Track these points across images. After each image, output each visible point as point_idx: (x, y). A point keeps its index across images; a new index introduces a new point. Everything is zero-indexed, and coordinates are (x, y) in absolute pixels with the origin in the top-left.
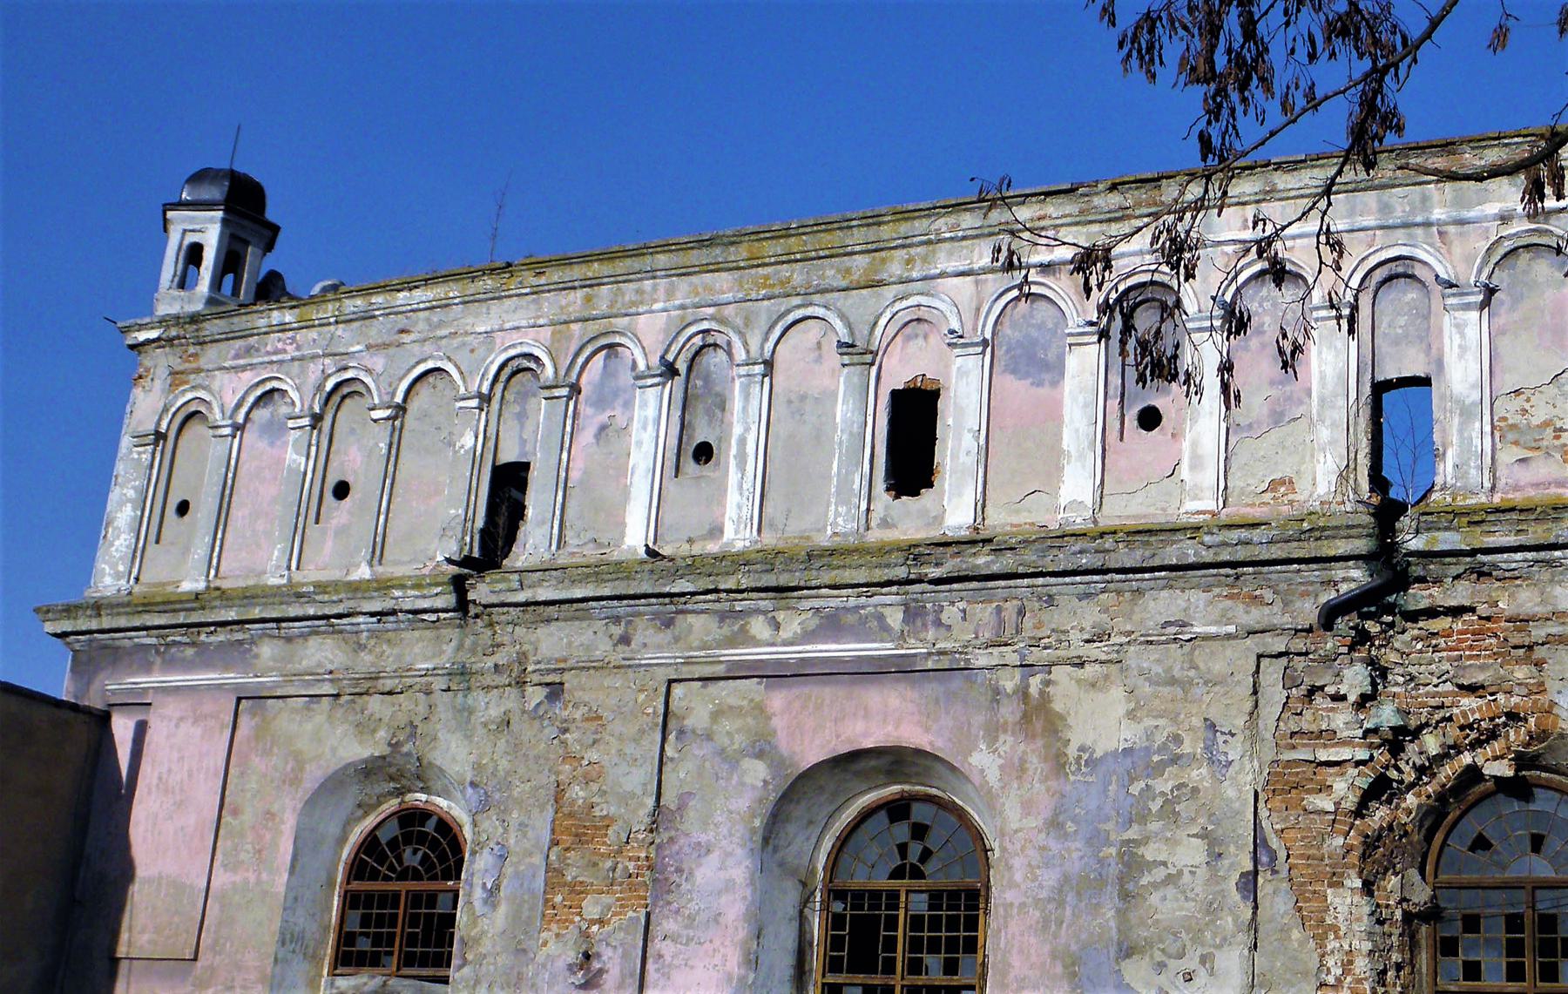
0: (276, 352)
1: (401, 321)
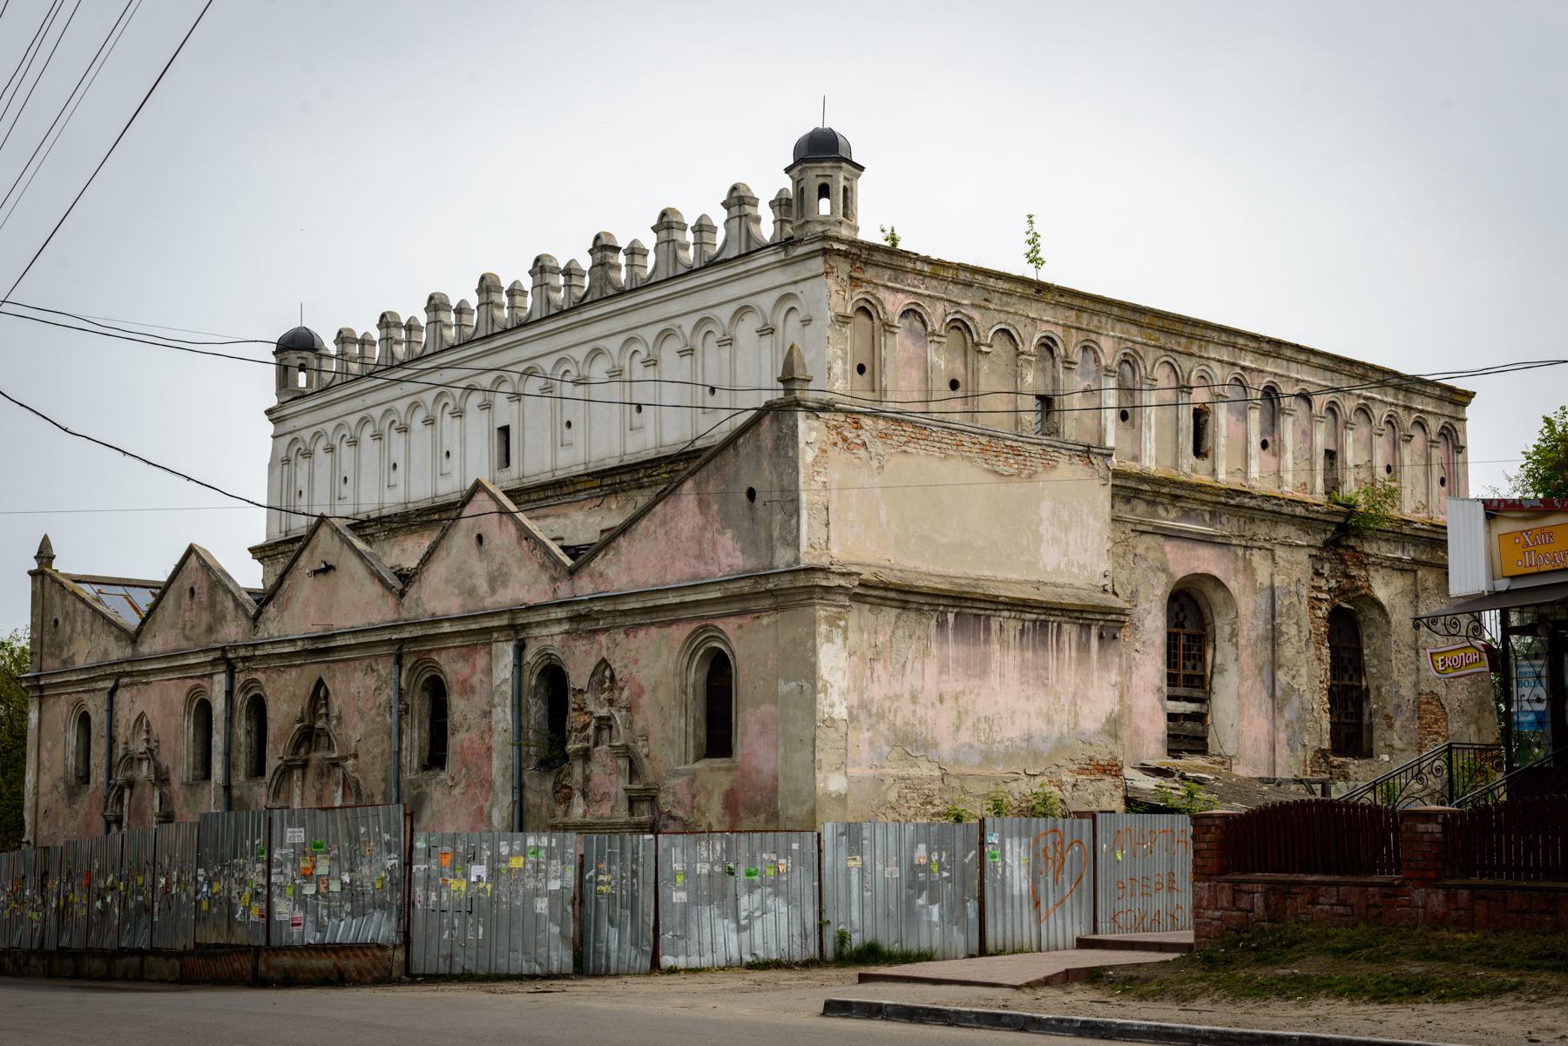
0: (914, 286)
1: (987, 296)
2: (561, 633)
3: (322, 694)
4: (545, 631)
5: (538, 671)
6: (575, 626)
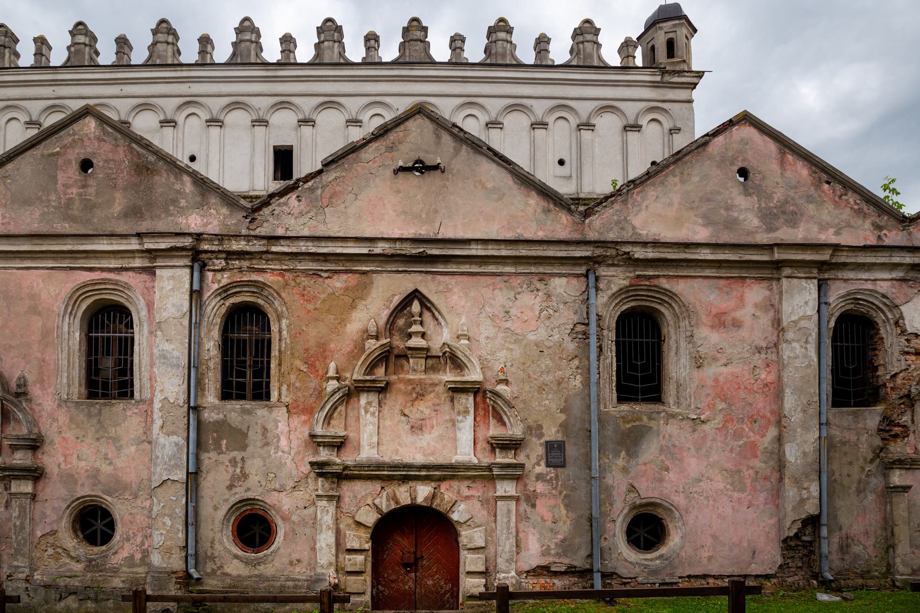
2: (892, 279)
3: (416, 307)
4: (865, 276)
5: (837, 314)
6: (912, 275)
